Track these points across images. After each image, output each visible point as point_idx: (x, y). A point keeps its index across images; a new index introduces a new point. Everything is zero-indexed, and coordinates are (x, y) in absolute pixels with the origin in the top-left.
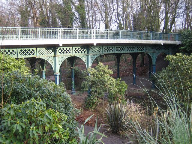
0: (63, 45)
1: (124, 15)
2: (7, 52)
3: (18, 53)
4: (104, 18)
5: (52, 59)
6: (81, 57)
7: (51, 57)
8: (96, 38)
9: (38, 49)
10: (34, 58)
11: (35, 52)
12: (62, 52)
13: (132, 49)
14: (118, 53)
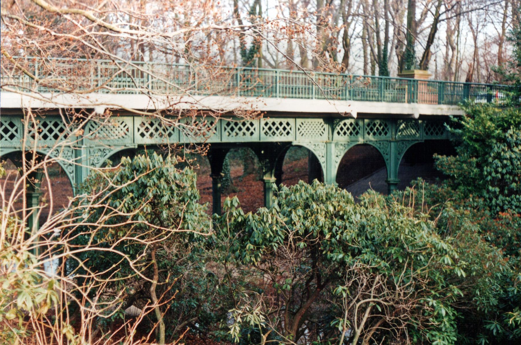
0: (359, 114)
1: (369, 48)
2: (6, 128)
3: (136, 130)
4: (376, 57)
5: (323, 147)
6: (313, 147)
7: (320, 144)
8: (281, 95)
9: (299, 121)
10: (290, 143)
11: (264, 129)
12: (270, 133)
13: (437, 130)
14: (434, 139)
